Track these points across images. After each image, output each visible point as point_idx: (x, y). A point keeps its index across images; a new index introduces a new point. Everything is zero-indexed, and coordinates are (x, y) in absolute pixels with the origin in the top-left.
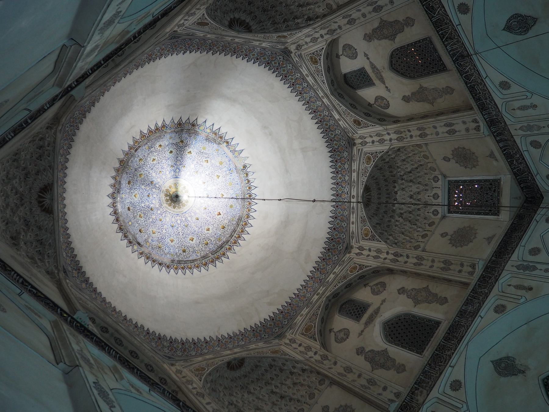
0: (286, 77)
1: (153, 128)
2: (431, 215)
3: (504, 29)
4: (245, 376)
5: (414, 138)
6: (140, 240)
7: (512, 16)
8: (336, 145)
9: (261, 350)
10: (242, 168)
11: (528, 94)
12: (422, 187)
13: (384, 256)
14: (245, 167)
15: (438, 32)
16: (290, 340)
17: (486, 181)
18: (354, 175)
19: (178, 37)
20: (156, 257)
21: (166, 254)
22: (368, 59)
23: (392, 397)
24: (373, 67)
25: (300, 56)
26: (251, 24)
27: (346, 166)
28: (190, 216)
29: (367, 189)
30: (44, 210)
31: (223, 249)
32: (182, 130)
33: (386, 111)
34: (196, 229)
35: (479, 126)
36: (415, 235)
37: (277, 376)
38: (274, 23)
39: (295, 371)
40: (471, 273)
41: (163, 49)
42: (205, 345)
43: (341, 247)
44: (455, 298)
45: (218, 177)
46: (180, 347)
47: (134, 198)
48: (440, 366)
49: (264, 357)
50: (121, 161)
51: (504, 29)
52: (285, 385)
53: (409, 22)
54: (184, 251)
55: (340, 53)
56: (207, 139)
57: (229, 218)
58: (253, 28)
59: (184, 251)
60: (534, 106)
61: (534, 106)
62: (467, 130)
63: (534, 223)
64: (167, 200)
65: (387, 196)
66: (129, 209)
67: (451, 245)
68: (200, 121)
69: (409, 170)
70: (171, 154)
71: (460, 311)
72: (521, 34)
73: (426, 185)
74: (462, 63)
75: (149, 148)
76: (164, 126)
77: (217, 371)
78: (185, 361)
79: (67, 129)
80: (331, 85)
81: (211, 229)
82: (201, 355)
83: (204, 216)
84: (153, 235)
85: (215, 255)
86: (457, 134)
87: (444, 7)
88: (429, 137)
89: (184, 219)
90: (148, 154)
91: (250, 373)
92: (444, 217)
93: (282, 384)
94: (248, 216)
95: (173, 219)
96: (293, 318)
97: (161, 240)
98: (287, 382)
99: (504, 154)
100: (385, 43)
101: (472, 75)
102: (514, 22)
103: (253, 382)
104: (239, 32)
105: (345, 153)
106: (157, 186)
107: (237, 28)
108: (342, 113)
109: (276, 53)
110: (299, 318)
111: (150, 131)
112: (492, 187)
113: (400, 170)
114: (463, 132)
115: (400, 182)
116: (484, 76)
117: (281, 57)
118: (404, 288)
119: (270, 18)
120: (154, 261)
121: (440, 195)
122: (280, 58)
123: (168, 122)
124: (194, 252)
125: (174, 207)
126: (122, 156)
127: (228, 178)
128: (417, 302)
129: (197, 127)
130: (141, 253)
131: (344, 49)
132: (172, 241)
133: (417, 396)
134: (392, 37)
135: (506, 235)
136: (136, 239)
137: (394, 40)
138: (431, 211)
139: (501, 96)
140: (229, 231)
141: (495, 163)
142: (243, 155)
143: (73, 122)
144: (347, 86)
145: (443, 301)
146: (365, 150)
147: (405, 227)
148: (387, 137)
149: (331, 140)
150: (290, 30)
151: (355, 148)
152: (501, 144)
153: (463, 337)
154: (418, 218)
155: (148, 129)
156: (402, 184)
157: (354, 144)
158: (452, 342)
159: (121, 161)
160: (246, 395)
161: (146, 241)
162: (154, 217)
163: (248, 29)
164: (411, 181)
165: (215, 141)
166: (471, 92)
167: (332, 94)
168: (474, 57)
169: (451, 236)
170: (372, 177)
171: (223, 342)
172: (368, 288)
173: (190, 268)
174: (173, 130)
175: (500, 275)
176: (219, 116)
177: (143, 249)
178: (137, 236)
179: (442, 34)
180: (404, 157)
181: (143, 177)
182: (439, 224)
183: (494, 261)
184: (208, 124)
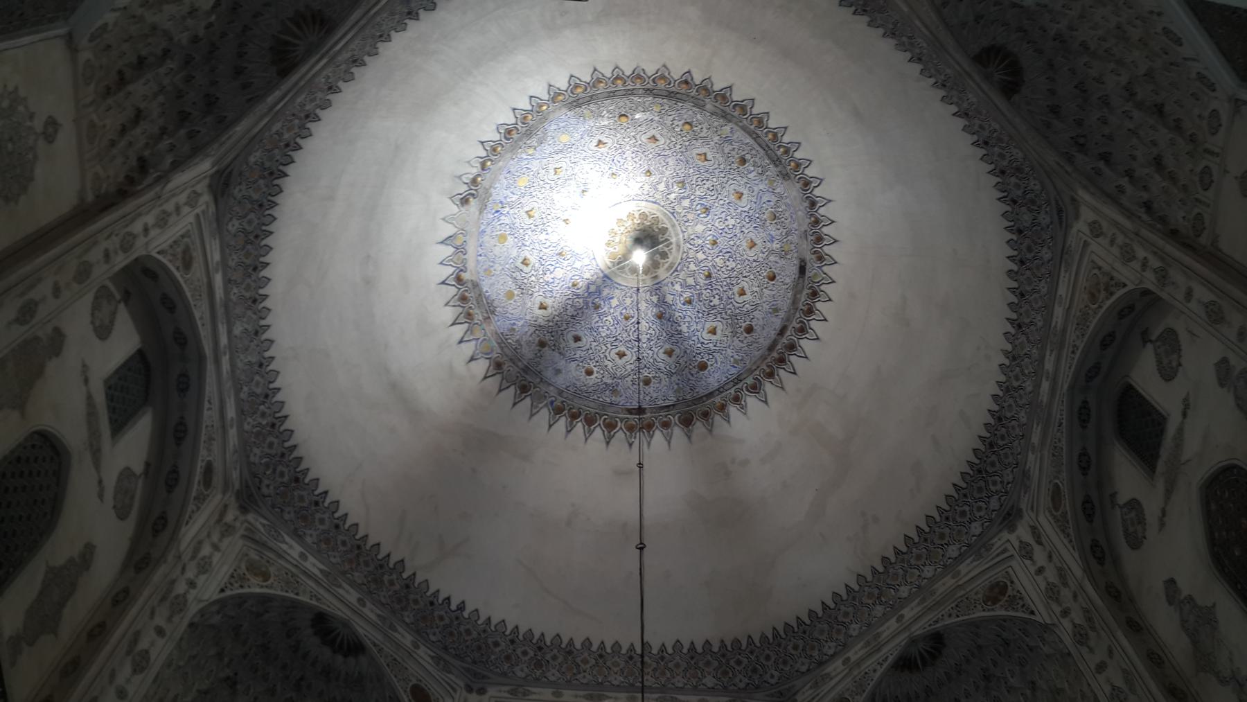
0: (273, 425)
1: (579, 427)
6: (793, 270)
14: (465, 201)
20: (805, 224)
21: (780, 196)
22: (100, 482)
24: (96, 453)
28: (657, 190)
31: (673, 89)
32: (526, 369)
34: (671, 161)
41: (508, 658)
47: (719, 331)
50: (687, 422)
55: (140, 483)
56: (490, 310)
59: (743, 161)
66: (749, 330)
68: (481, 367)
70: (581, 334)
76: (558, 411)
79: (776, 674)
81: (649, 135)
83: (630, 165)
85: (701, 97)
89: (672, 196)
90: (622, 378)
94: (555, 96)
95: (690, 217)
104: (346, 624)
106: (655, 299)
109: (273, 506)
111: (590, 421)
115: (184, 38)
117: (265, 490)
120: (817, 222)
122: (268, 486)
123: (544, 414)
124: (727, 140)
125: (664, 230)
127: (514, 198)
132: (740, 195)
142: (449, 230)
149: (261, 206)
159: (687, 422)
167: (202, 358)
173: (775, 135)
174: (544, 388)
176: (436, 358)
177: (809, 257)
178: (788, 280)
181: (667, 346)
184: (468, 349)
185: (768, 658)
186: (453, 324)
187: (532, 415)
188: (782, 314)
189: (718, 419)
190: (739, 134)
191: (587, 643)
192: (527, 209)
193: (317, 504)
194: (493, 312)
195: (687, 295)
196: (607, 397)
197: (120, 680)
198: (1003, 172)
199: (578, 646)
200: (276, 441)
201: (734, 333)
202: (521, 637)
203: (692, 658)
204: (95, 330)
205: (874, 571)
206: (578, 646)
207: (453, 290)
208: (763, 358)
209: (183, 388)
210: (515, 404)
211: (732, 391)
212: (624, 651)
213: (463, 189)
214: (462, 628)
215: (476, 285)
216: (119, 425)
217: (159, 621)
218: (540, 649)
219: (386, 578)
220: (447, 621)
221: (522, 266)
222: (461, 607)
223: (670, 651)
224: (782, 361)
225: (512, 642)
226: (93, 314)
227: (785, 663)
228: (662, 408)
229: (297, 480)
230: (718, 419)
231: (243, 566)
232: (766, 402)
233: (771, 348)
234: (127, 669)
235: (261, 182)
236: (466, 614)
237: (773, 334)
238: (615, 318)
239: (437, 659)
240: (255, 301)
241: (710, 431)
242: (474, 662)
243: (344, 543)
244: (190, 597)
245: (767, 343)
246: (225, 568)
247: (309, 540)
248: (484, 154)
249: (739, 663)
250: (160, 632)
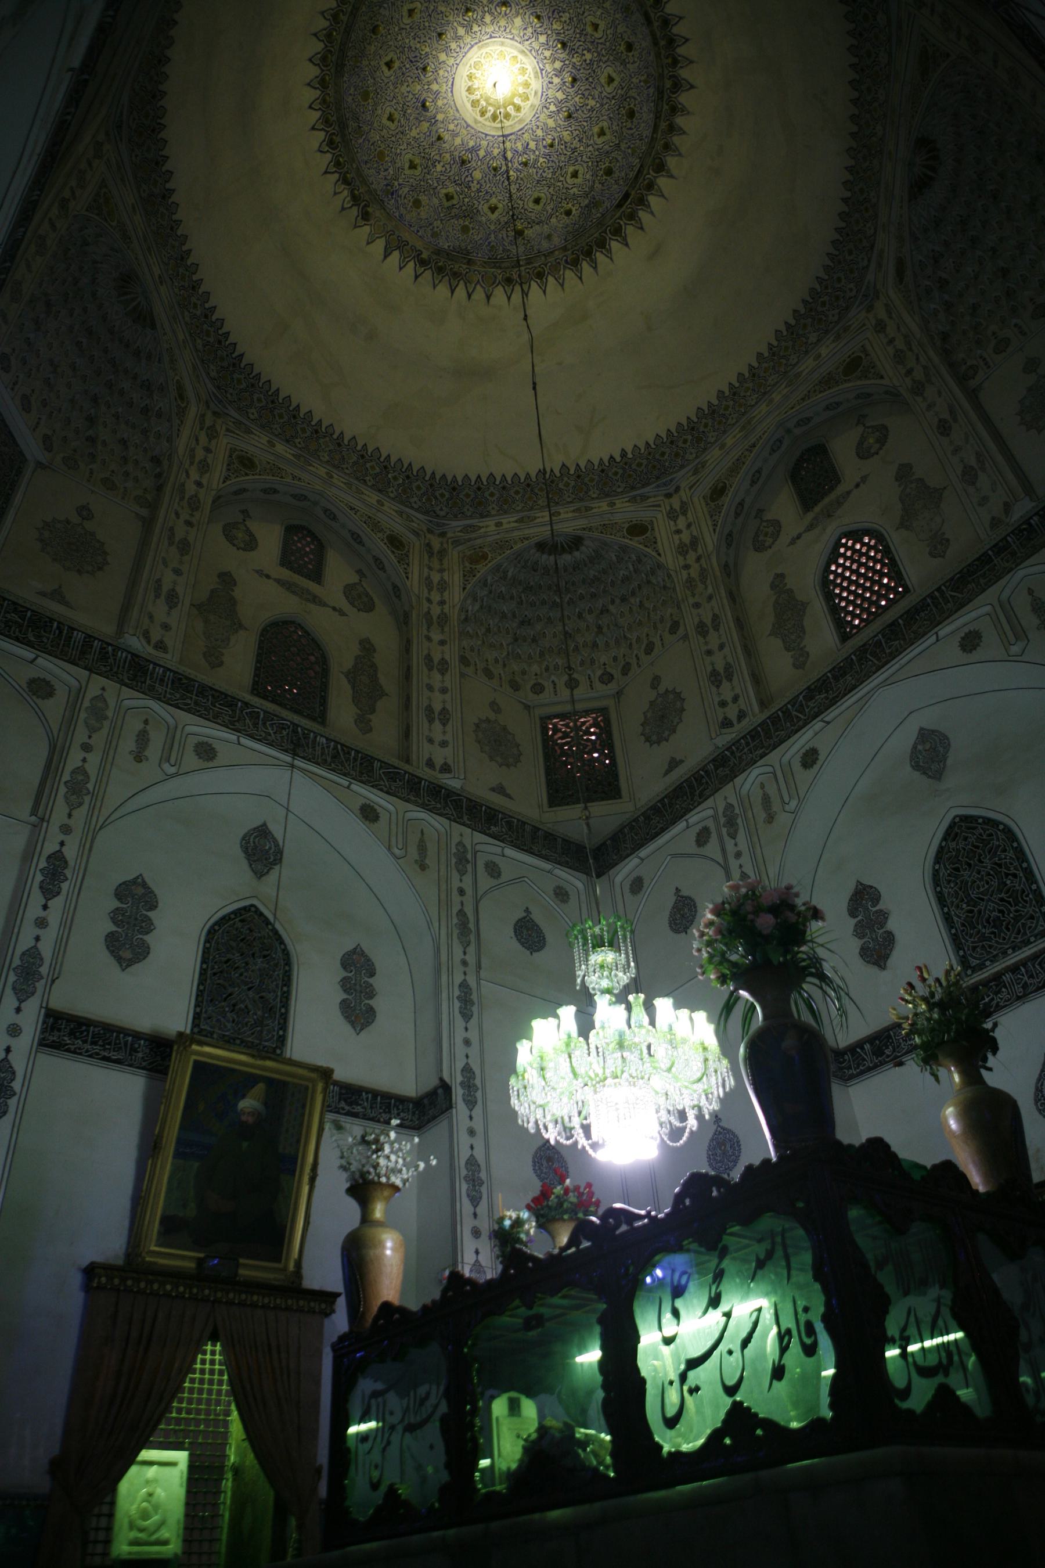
0: (408, 477)
1: (600, 257)
3: (265, 825)
8: (239, 381)
10: (370, 210)
11: (173, 770)
15: (357, 752)
19: (658, 486)
22: (334, 609)
24: (315, 600)
41: (677, 455)
45: (413, 166)
47: (614, 75)
51: (265, 825)
53: (364, 723)
58: (533, 551)
74: (285, 733)
75: (594, 204)
79: (852, 285)
90: (592, 188)
99: (52, 620)
100: (349, 663)
101: (256, 725)
102: (270, 848)
111: (602, 244)
117: (442, 513)
131: (367, 595)
134: (352, 676)
137: (347, 674)
142: (380, 245)
143: (837, 298)
149: (253, 385)
152: (78, 636)
155: (610, 251)
166: (226, 695)
179: (349, 753)
184: (479, 294)
185: (839, 280)
186: (452, 292)
187: (562, 285)
189: (676, 140)
191: (720, 394)
192: (407, 165)
193: (479, 489)
194: (468, 253)
196: (596, 214)
197: (437, 685)
199: (715, 402)
200: (419, 483)
202: (676, 434)
203: (792, 333)
204: (244, 550)
205: (853, 135)
206: (715, 402)
207: (428, 274)
210: (544, 292)
211: (666, 107)
212: (747, 375)
213: (354, 211)
214: (634, 466)
215: (438, 252)
216: (317, 575)
217: (436, 637)
218: (693, 429)
219: (561, 486)
220: (621, 471)
221: (450, 203)
222: (624, 454)
223: (775, 343)
225: (672, 442)
226: (234, 545)
228: (637, 177)
229: (454, 489)
230: (676, 140)
231: (467, 564)
232: (692, 87)
234: (438, 676)
235: (236, 376)
236: (630, 456)
238: (545, 155)
239: (633, 500)
240: (317, 432)
241: (680, 155)
242: (658, 478)
243: (517, 492)
244: (446, 610)
246: (456, 577)
247: (493, 512)
248: (337, 176)
249: (824, 304)
250: (442, 643)
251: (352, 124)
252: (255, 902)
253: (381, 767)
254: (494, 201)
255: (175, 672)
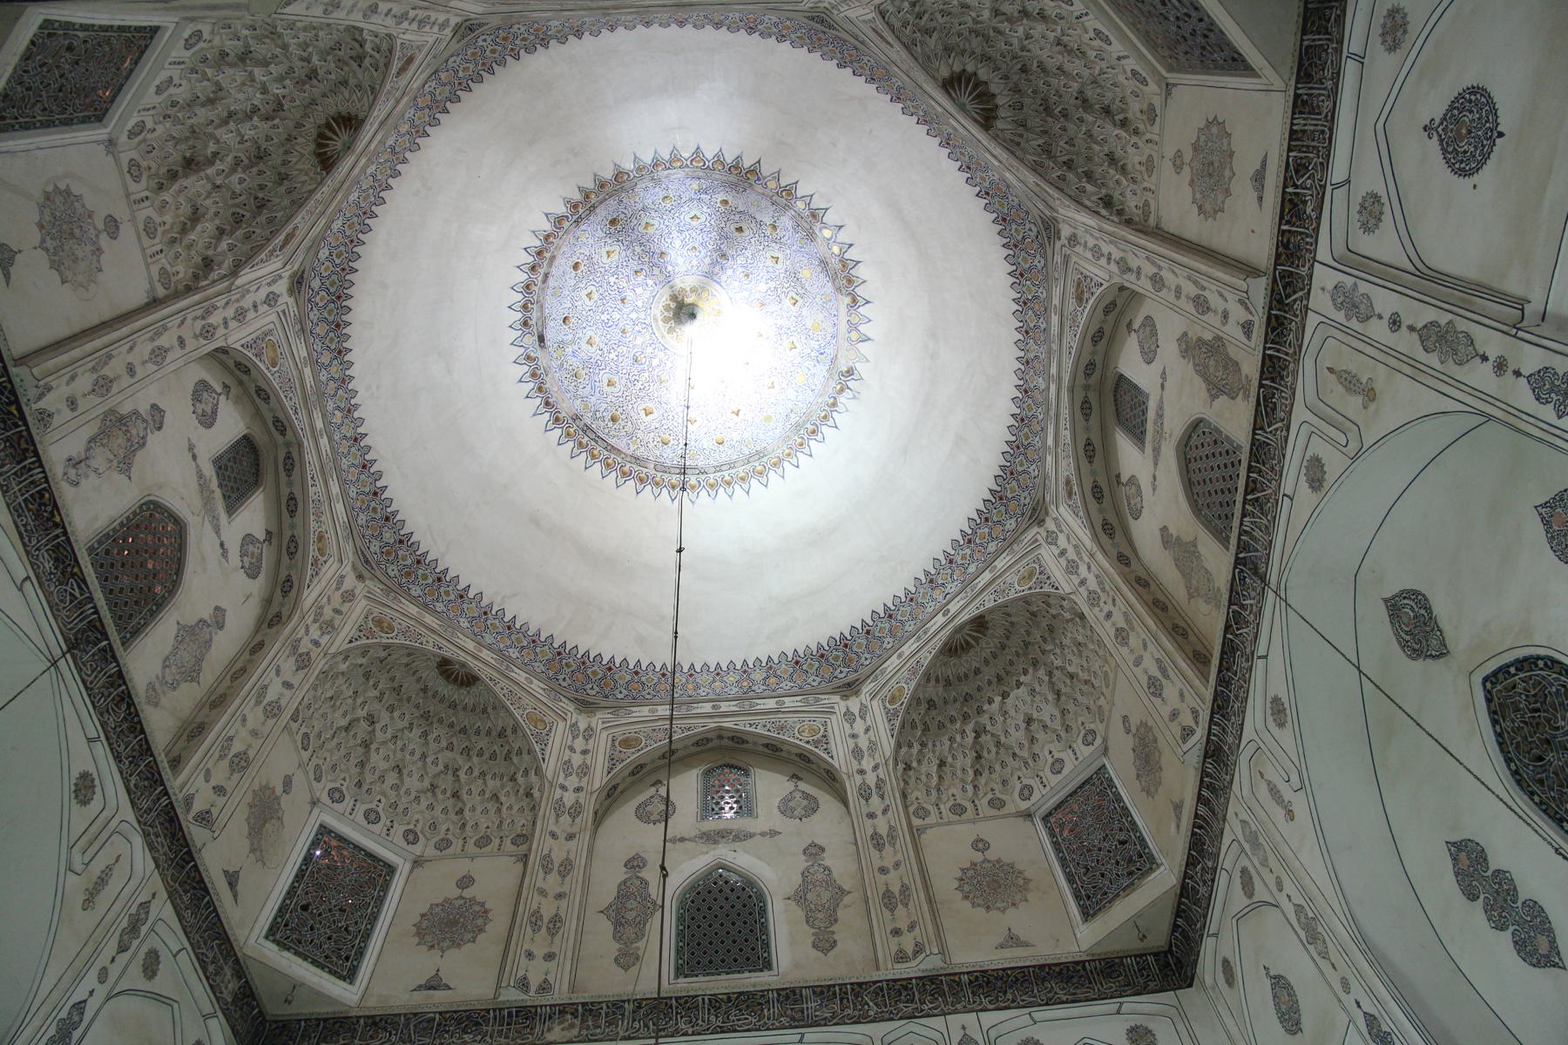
2: (1018, 786)
3: (1386, 601)
4: (453, 706)
5: (1108, 624)
6: (550, 336)
7: (1416, 593)
8: (1013, 491)
9: (521, 693)
11: (1295, 778)
12: (1057, 725)
13: (867, 764)
14: (850, 372)
16: (589, 728)
17: (1142, 840)
18: (987, 576)
19: (830, 27)
23: (535, 981)
25: (1066, 259)
26: (1002, 113)
27: (992, 547)
29: (980, 623)
30: (319, 155)
33: (1131, 521)
35: (1192, 732)
36: (953, 790)
37: (493, 756)
38: (1047, 150)
39: (521, 780)
40: (901, 957)
42: (452, 597)
43: (844, 675)
44: (850, 960)
46: (409, 562)
48: (646, 1026)
49: (508, 710)
50: (619, 175)
51: (1386, 601)
52: (485, 783)
54: (614, 419)
55: (1136, 326)
57: (746, 435)
58: (999, 124)
59: (614, 419)
60: (1290, 815)
61: (1290, 815)
62: (1174, 715)
63: (1110, 1006)
64: (667, 308)
65: (1002, 673)
66: (576, 266)
67: (959, 874)
69: (1071, 669)
71: (793, 990)
72: (1403, 648)
73: (1068, 729)
77: (409, 655)
78: (388, 590)
80: (1081, 369)
82: (426, 606)
84: (585, 346)
86: (1157, 701)
87: (1288, 430)
88: (1125, 650)
90: (691, 200)
91: (465, 708)
92: (1028, 815)
93: (483, 774)
96: (636, 701)
97: (592, 365)
98: (491, 783)
99: (1193, 834)
102: (1412, 609)
103: (451, 725)
105: (1013, 521)
107: (965, 99)
108: (1061, 442)
110: (645, 711)
112: (1139, 862)
113: (1058, 651)
114: (1166, 711)
115: (1042, 673)
116: (1261, 651)
118: (823, 850)
119: (1046, 132)
121: (1065, 772)
124: (630, 435)
126: (628, 165)
128: (799, 897)
129: (819, 225)
130: (528, 358)
132: (610, 384)
133: (561, 1023)
135: (1042, 967)
136: (544, 326)
138: (1025, 781)
139: (1260, 725)
140: (724, 458)
141: (1173, 827)
143: (505, 39)
144: (1107, 403)
145: (824, 943)
146: (1042, 551)
147: (960, 757)
148: (1083, 570)
150: (1062, 190)
151: (1035, 529)
153: (735, 1031)
154: (998, 767)
156: (1040, 681)
157: (1041, 523)
158: (713, 1018)
160: (416, 732)
161: (561, 345)
162: (616, 316)
163: (987, 119)
164: (1058, 694)
165: (834, 278)
167: (1072, 390)
168: (1270, 595)
169: (986, 860)
170: (1003, 609)
171: (486, 619)
172: (790, 786)
173: (593, 457)
175: (928, 1016)
179: (1254, 481)
180: (1080, 639)
182: (1004, 817)
183: (959, 984)
185: (493, 51)
188: (549, 292)
190: (621, 445)
195: (641, 278)
198: (419, 562)
201: (590, 258)
208: (558, 248)
209: (1090, 367)
215: (839, 289)
224: (539, 253)
227: (474, 54)
230: (590, 185)
233: (553, 258)
237: (554, 271)
245: (556, 263)
251: (794, 419)
252: (1477, 679)
253: (1262, 428)
254: (770, 263)
255: (1212, 712)
